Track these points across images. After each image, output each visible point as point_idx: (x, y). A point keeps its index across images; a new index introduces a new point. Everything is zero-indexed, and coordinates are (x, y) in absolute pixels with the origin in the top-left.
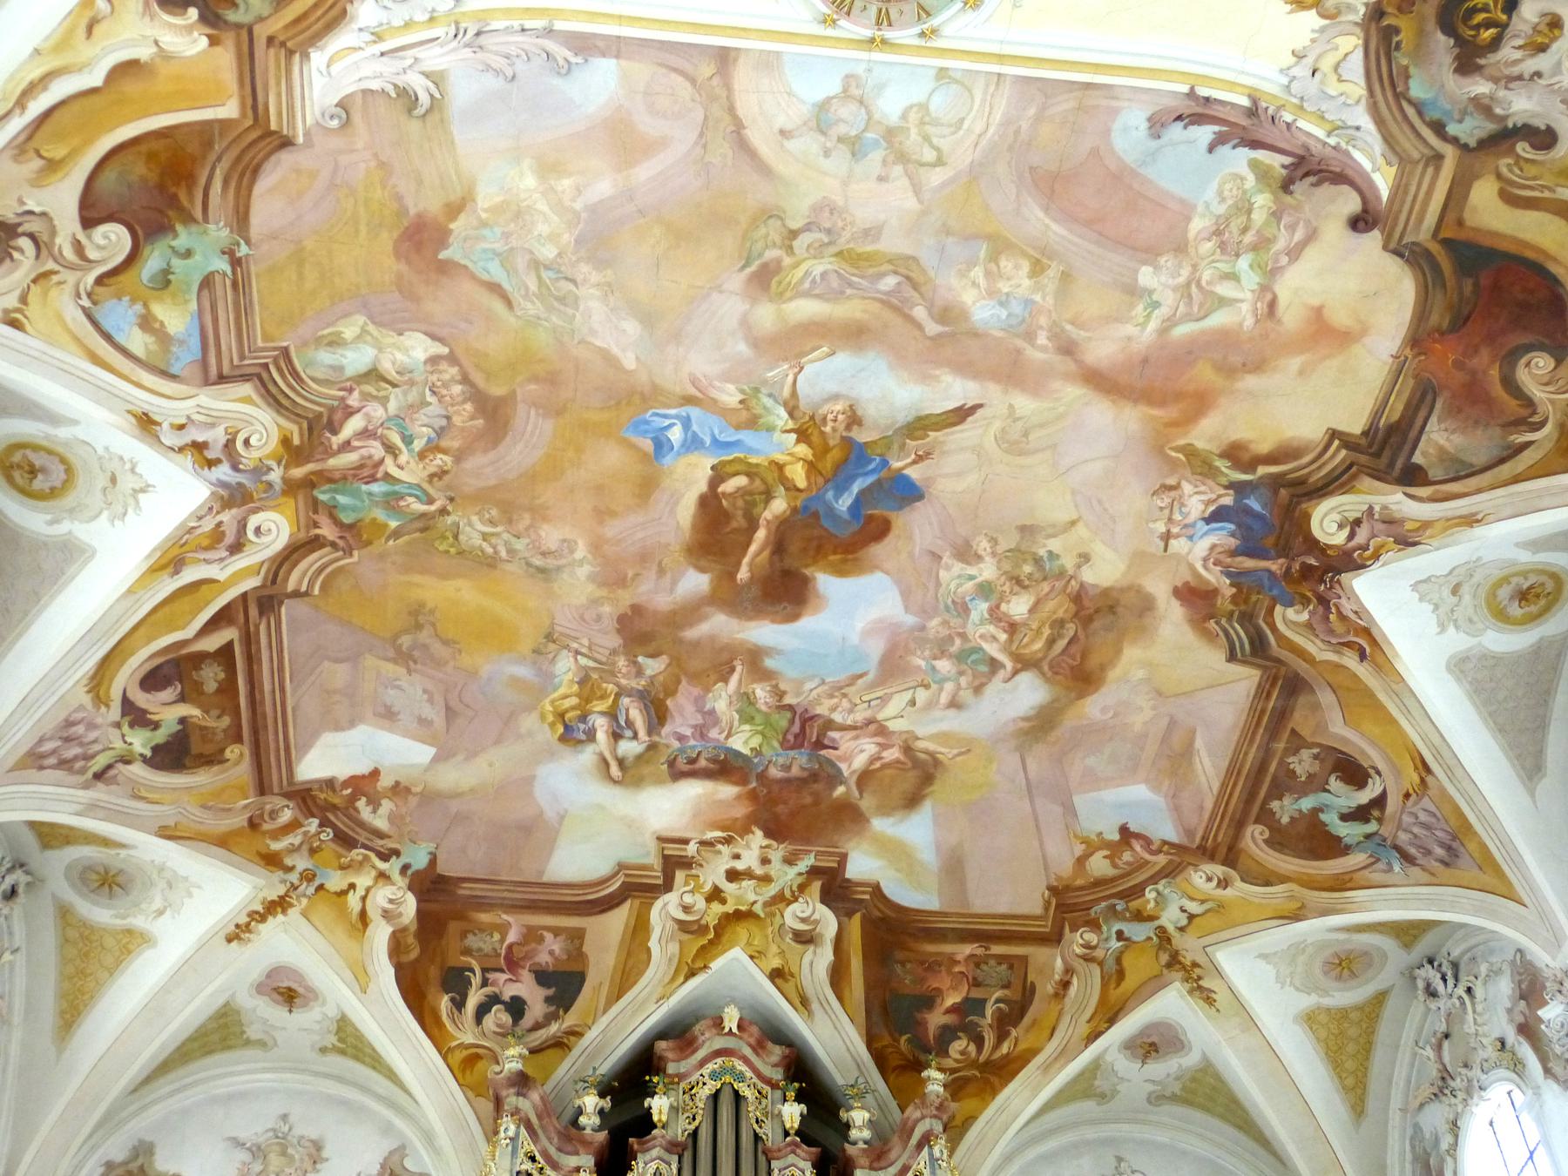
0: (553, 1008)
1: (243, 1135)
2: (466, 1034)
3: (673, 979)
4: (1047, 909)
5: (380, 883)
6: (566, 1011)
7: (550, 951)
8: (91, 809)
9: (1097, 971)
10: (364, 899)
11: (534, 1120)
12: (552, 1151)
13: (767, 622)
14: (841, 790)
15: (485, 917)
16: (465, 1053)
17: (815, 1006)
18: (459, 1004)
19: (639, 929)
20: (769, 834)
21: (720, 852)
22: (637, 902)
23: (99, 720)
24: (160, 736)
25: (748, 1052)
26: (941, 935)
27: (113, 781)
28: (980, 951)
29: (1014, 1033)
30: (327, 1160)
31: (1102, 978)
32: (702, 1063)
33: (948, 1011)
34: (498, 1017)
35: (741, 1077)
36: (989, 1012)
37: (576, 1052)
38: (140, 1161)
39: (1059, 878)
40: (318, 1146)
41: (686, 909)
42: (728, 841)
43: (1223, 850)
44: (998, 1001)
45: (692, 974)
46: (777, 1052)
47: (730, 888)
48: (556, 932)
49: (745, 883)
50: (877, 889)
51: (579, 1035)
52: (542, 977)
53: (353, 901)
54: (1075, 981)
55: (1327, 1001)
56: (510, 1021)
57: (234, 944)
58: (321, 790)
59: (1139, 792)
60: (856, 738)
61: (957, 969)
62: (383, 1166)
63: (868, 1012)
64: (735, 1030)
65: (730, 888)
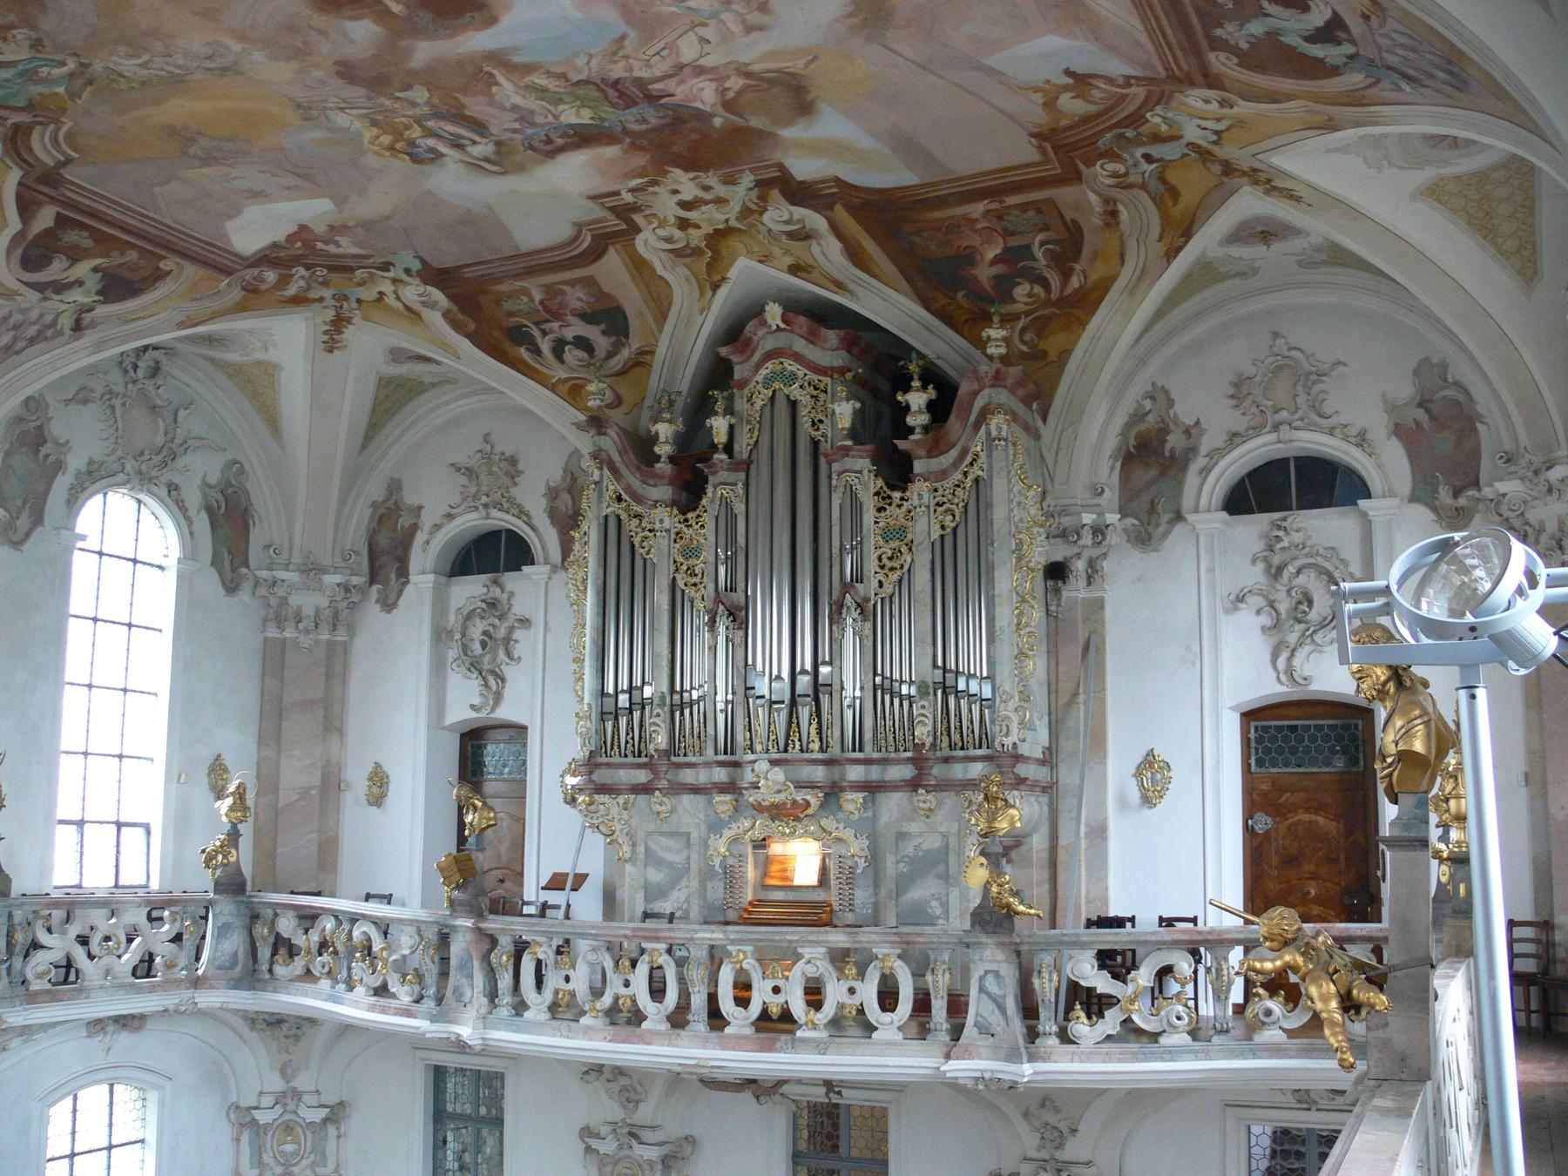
0: (614, 339)
1: (461, 458)
2: (560, 373)
3: (702, 293)
4: (1044, 153)
5: (401, 286)
6: (627, 336)
7: (576, 298)
8: (99, 346)
9: (1143, 196)
10: (398, 298)
11: (616, 458)
12: (636, 484)
13: (470, 33)
14: (718, 122)
15: (504, 287)
16: (570, 383)
17: (851, 286)
18: (537, 352)
19: (639, 266)
20: (686, 169)
21: (656, 193)
22: (618, 247)
23: (25, 305)
24: (93, 282)
25: (800, 345)
26: (943, 202)
27: (93, 324)
28: (993, 206)
29: (1078, 267)
30: (522, 472)
31: (1154, 200)
32: (758, 366)
33: (993, 262)
34: (572, 355)
35: (793, 377)
36: (1039, 253)
37: (656, 366)
38: (394, 497)
39: (1036, 125)
40: (513, 461)
41: (668, 240)
42: (655, 183)
43: (1198, 77)
44: (1042, 244)
45: (716, 287)
46: (832, 336)
47: (692, 215)
48: (572, 283)
49: (704, 208)
50: (839, 182)
51: (653, 353)
52: (588, 318)
53: (390, 300)
54: (1121, 207)
55: (1449, 171)
56: (586, 355)
57: (336, 351)
58: (273, 252)
59: (1052, 42)
60: (682, 82)
61: (980, 226)
62: (565, 470)
63: (909, 280)
64: (782, 326)
65: (692, 215)
